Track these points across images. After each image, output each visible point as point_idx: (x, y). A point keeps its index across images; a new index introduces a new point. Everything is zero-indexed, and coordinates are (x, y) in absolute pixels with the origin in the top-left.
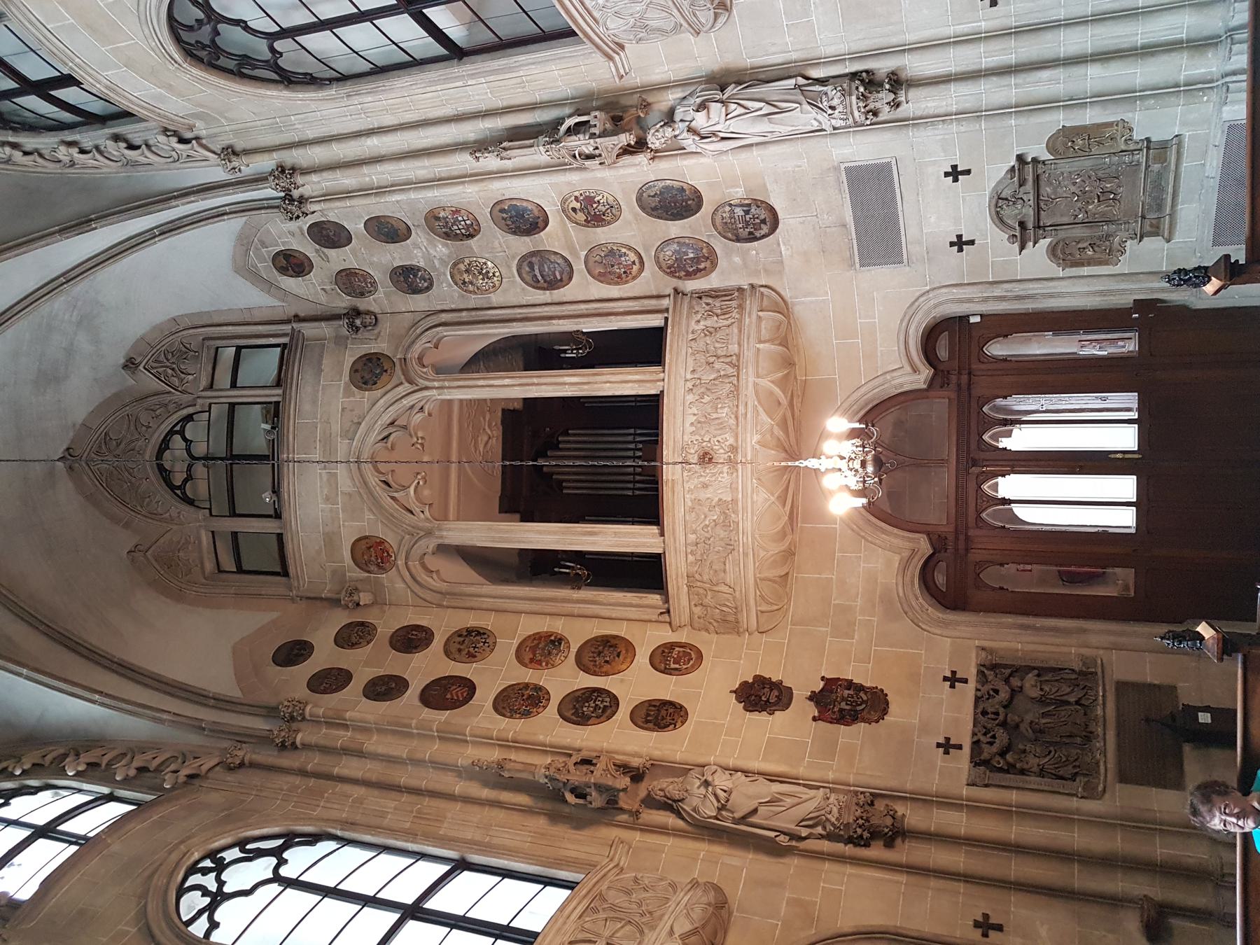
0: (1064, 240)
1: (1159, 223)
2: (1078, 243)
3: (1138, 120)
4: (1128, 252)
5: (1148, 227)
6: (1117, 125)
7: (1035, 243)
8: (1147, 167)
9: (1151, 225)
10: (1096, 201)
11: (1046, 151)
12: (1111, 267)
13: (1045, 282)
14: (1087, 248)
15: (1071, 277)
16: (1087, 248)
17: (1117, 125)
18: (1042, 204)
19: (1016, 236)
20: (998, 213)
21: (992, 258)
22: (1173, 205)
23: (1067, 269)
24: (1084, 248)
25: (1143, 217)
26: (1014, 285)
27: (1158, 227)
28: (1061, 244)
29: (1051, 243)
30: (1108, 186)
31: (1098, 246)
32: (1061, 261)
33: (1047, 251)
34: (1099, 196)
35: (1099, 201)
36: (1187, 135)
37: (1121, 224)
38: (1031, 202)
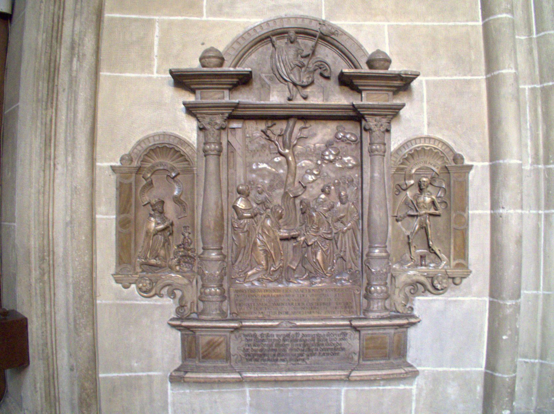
0: (189, 171)
1: (218, 357)
2: (177, 200)
3: (463, 302)
4: (146, 302)
5: (207, 338)
6: (458, 266)
7: (190, 110)
8: (355, 329)
9: (212, 345)
10: (284, 233)
11: (410, 135)
12: (113, 270)
13: (88, 126)
14: (164, 219)
15: (93, 183)
16: (164, 219)
17: (458, 266)
18: (281, 126)
19: (221, 65)
20: (282, 33)
21: (161, 22)
22: (254, 382)
23: (113, 177)
24: (162, 213)
25: (236, 329)
26: (89, 59)
27: (206, 357)
28: (179, 165)
29: (184, 142)
30: (319, 257)
31: (167, 241)
32: (135, 164)
33: (165, 134)
34: (294, 238)
35: (282, 239)
36: (414, 387)
37: (220, 286)
38: (299, 101)
